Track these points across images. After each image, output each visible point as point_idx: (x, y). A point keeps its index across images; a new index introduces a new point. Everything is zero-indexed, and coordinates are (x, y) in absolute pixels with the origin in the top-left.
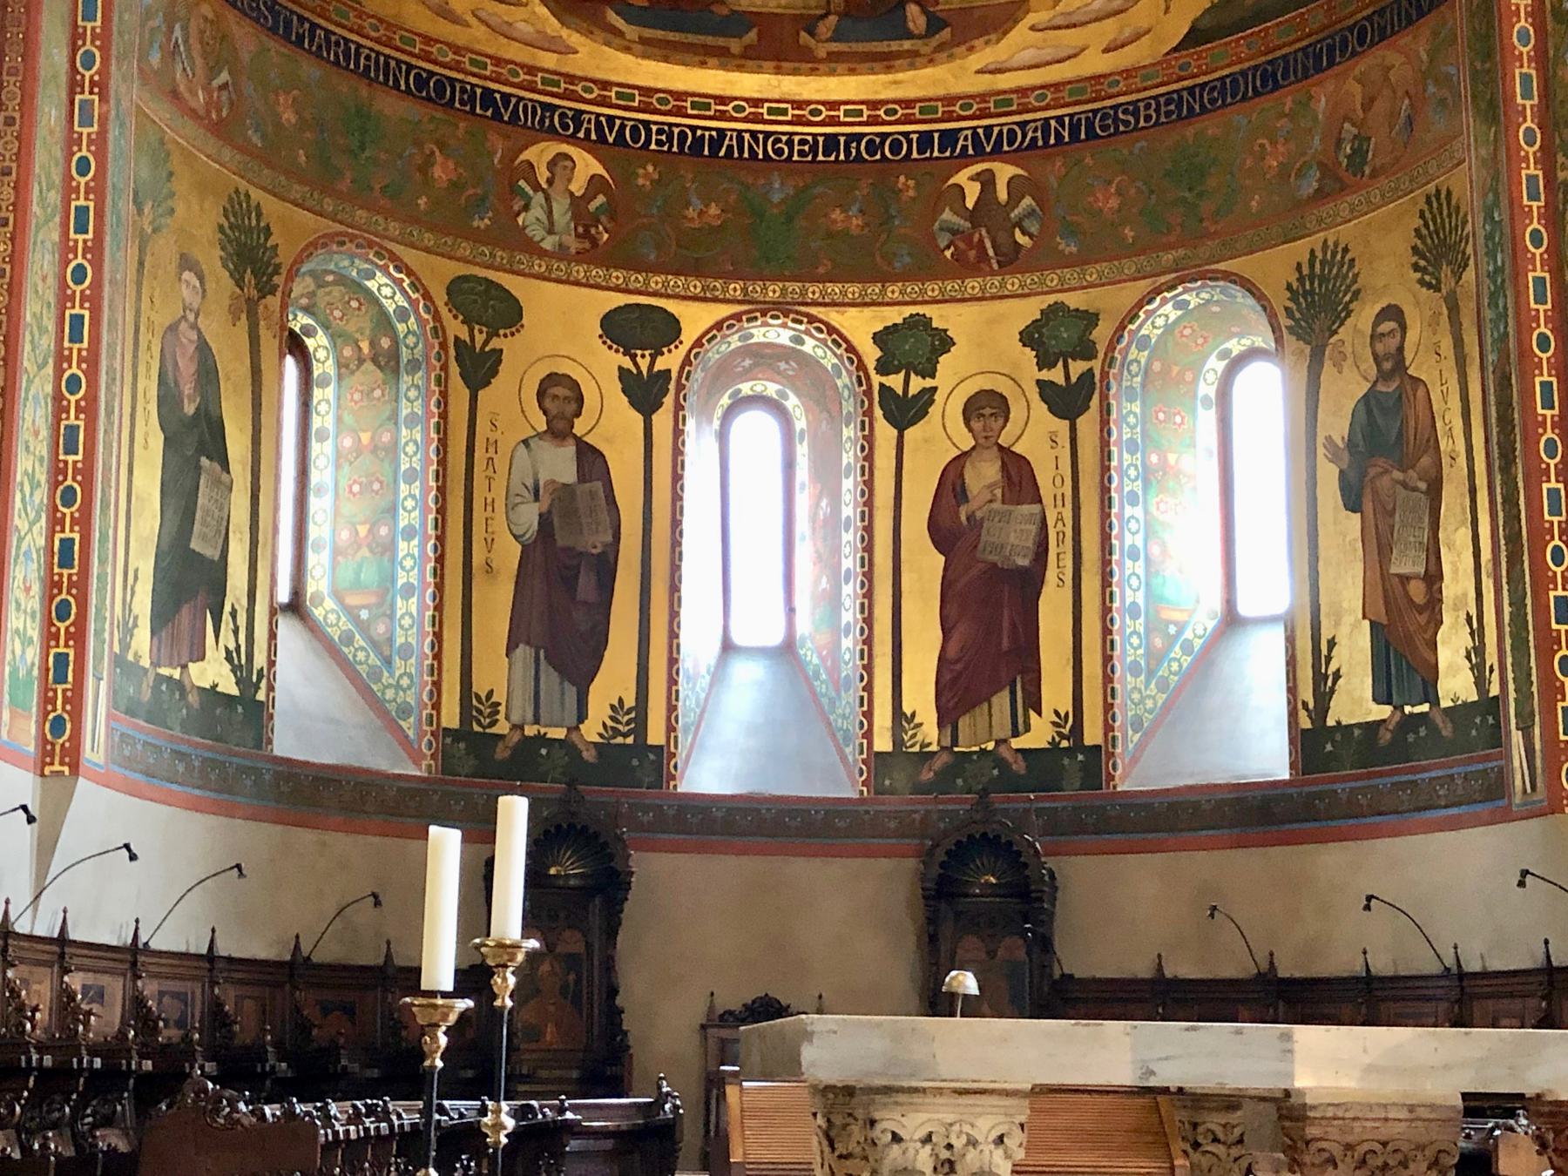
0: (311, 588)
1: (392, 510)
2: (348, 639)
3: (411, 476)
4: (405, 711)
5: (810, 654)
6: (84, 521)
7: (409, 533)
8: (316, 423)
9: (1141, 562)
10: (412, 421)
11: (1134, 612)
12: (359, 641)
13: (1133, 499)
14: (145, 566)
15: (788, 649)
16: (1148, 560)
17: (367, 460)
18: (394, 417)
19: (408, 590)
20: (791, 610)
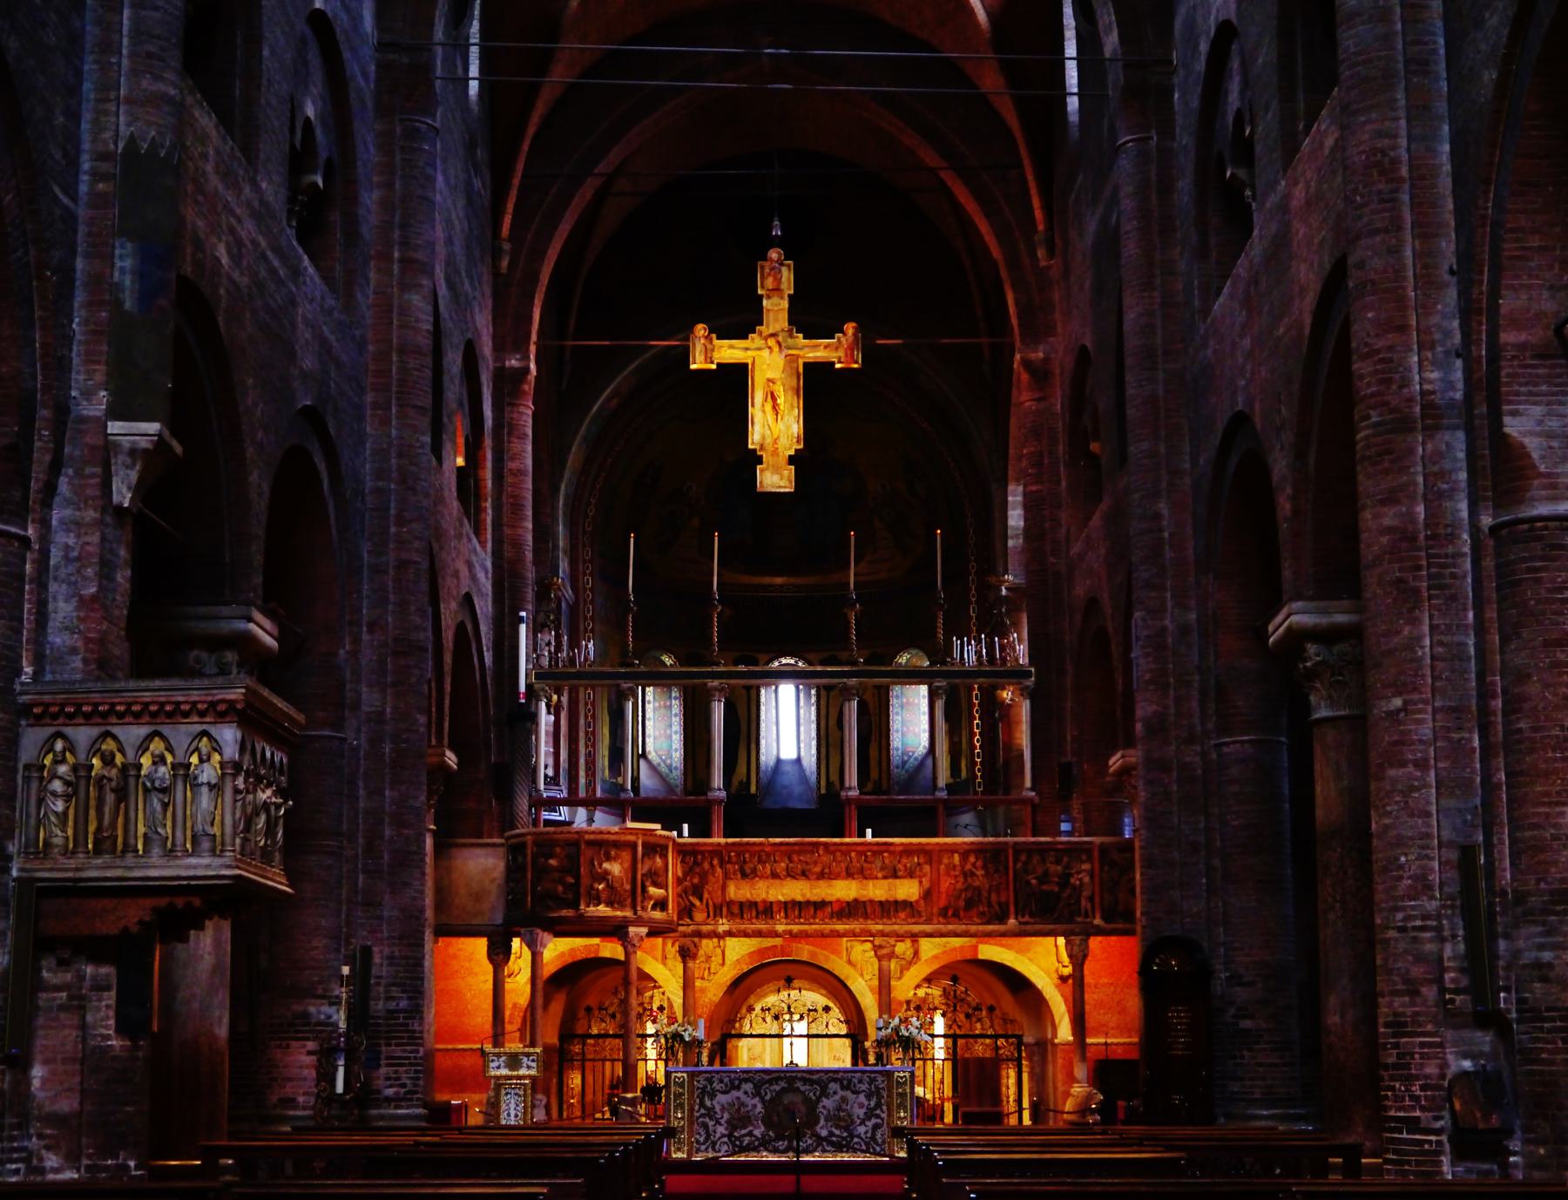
0: (648, 749)
1: (671, 726)
2: (659, 765)
3: (676, 715)
4: (677, 786)
5: (805, 762)
6: (594, 746)
7: (676, 733)
8: (647, 698)
9: (900, 733)
10: (676, 698)
11: (897, 749)
12: (663, 765)
13: (897, 714)
14: (606, 753)
15: (798, 760)
16: (903, 734)
17: (663, 711)
18: (670, 697)
19: (676, 750)
20: (799, 748)
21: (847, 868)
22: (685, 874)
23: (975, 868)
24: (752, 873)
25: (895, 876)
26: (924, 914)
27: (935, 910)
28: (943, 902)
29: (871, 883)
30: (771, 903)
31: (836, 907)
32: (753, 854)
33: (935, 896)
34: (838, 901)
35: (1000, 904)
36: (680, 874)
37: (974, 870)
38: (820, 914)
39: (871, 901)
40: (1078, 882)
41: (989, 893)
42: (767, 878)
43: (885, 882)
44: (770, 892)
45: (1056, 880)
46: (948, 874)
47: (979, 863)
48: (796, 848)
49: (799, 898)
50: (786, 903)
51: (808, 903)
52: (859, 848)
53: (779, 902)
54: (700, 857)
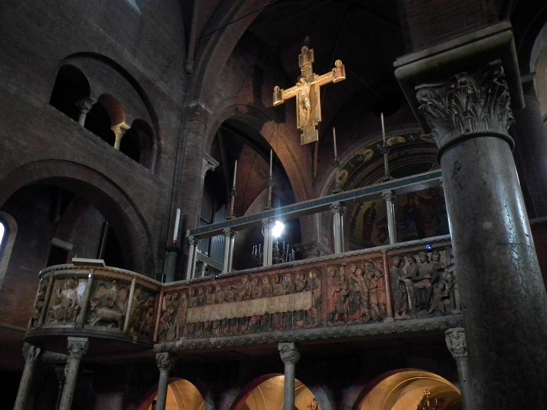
21: (263, 290)
22: (168, 307)
23: (356, 276)
24: (203, 301)
25: (296, 291)
26: (316, 320)
27: (325, 316)
28: (331, 308)
29: (276, 299)
30: (212, 322)
31: (253, 321)
32: (205, 289)
33: (324, 306)
34: (255, 316)
35: (378, 305)
36: (164, 308)
37: (354, 278)
38: (243, 328)
39: (278, 313)
40: (449, 276)
41: (369, 296)
42: (212, 304)
43: (286, 297)
44: (212, 314)
45: (428, 276)
46: (334, 284)
47: (359, 272)
48: (231, 279)
49: (229, 316)
50: (221, 320)
51: (235, 319)
52: (270, 273)
53: (217, 320)
54: (176, 294)
